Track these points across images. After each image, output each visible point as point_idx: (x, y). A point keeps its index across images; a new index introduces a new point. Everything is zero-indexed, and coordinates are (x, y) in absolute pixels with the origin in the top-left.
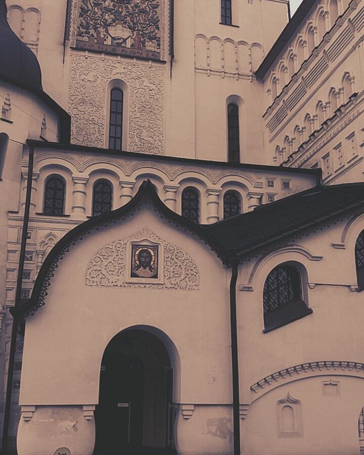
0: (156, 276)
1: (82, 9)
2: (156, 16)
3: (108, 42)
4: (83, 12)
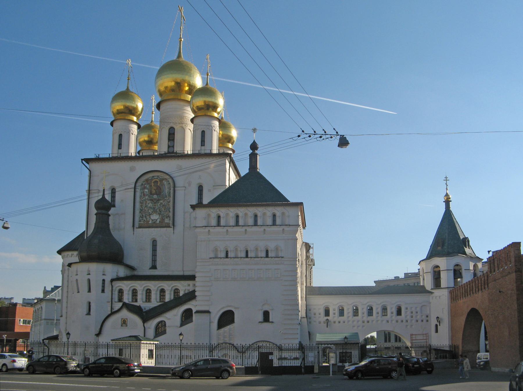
0: (127, 326)
1: (141, 209)
2: (169, 207)
3: (150, 222)
4: (141, 211)
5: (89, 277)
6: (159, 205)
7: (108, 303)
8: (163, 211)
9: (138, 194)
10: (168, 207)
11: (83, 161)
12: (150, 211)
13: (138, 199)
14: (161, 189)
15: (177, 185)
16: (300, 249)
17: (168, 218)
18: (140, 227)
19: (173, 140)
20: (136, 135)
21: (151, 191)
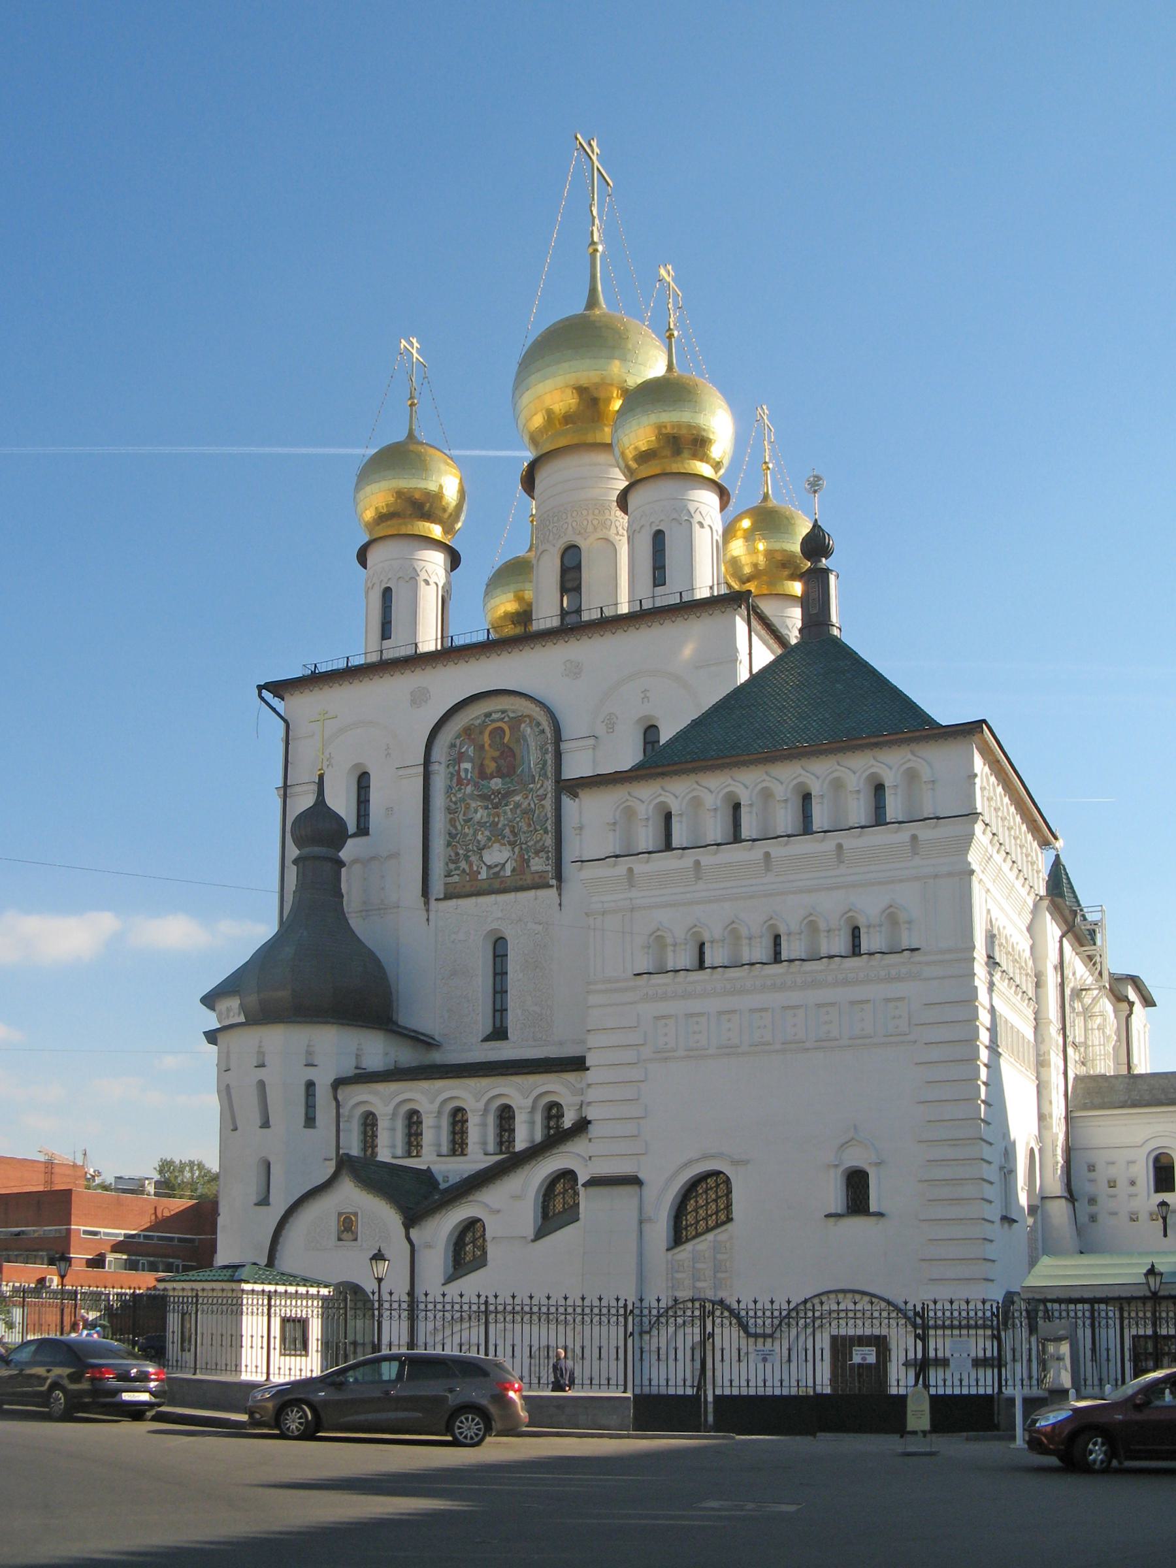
3: (483, 875)
5: (262, 1074)
6: (511, 809)
7: (327, 1163)
8: (525, 833)
9: (439, 783)
10: (539, 816)
11: (265, 693)
12: (479, 837)
13: (439, 801)
14: (514, 755)
15: (565, 735)
16: (1029, 929)
17: (542, 854)
18: (448, 897)
19: (578, 589)
20: (441, 585)
21: (482, 765)
